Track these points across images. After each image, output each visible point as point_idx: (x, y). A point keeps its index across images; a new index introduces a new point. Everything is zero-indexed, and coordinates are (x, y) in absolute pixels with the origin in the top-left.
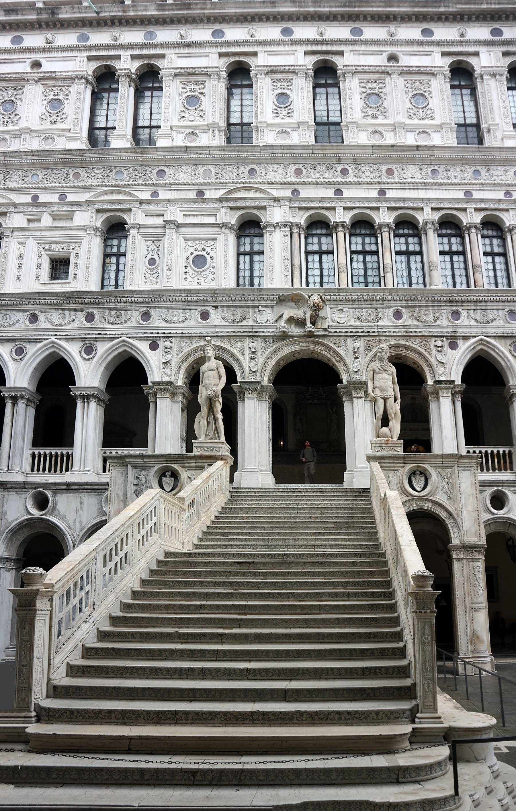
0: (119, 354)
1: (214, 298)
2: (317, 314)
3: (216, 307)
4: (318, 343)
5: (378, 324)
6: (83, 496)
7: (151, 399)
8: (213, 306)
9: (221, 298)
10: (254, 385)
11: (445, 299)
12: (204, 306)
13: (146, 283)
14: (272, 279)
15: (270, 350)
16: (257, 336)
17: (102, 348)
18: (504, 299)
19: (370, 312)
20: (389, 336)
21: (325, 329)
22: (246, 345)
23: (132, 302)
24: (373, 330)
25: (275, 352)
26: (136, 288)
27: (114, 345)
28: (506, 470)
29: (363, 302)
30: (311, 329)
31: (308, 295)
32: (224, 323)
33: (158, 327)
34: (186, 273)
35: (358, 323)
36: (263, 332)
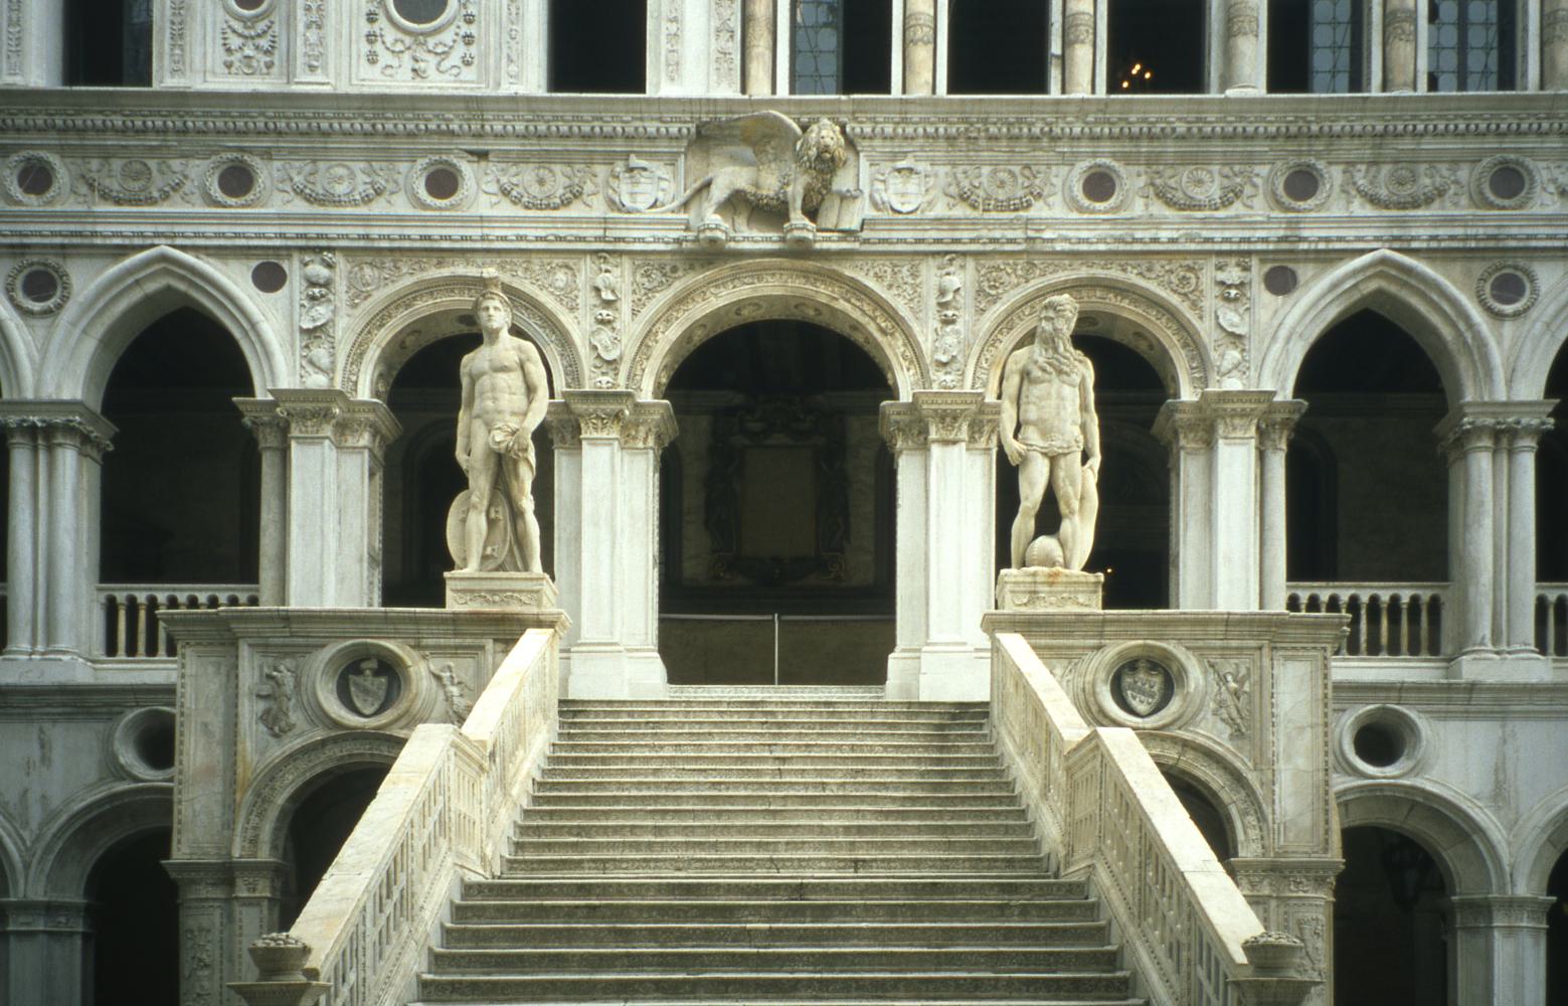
0: (149, 299)
1: (475, 126)
2: (827, 185)
3: (482, 155)
4: (836, 278)
5: (1032, 213)
6: (47, 726)
7: (268, 440)
8: (471, 153)
9: (498, 127)
10: (613, 407)
11: (1272, 129)
12: (439, 151)
13: (229, 65)
14: (675, 68)
15: (662, 298)
16: (621, 253)
17: (85, 280)
18: (1483, 126)
19: (1003, 175)
20: (1063, 253)
21: (848, 234)
22: (581, 280)
23: (185, 131)
24: (1010, 234)
25: (681, 300)
26: (198, 85)
27: (129, 272)
28: (1414, 650)
29: (983, 143)
30: (805, 234)
31: (798, 121)
32: (506, 209)
33: (283, 217)
34: (371, 38)
35: (961, 211)
36: (642, 240)
